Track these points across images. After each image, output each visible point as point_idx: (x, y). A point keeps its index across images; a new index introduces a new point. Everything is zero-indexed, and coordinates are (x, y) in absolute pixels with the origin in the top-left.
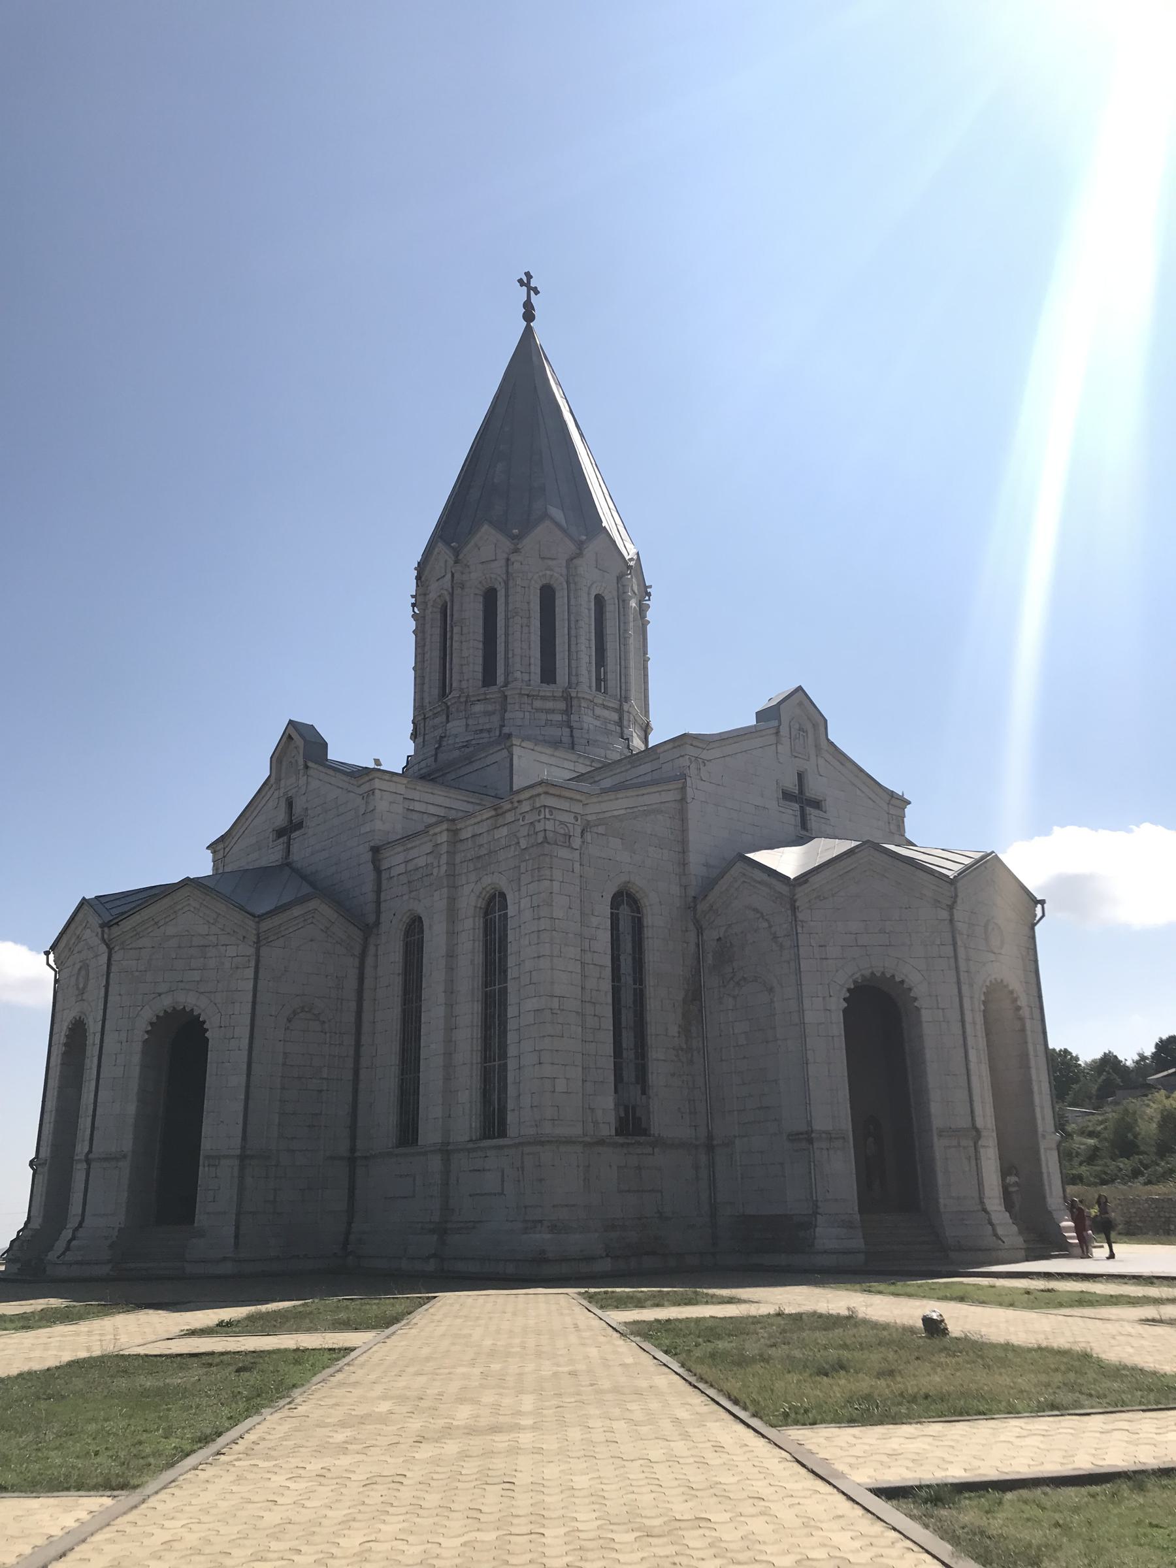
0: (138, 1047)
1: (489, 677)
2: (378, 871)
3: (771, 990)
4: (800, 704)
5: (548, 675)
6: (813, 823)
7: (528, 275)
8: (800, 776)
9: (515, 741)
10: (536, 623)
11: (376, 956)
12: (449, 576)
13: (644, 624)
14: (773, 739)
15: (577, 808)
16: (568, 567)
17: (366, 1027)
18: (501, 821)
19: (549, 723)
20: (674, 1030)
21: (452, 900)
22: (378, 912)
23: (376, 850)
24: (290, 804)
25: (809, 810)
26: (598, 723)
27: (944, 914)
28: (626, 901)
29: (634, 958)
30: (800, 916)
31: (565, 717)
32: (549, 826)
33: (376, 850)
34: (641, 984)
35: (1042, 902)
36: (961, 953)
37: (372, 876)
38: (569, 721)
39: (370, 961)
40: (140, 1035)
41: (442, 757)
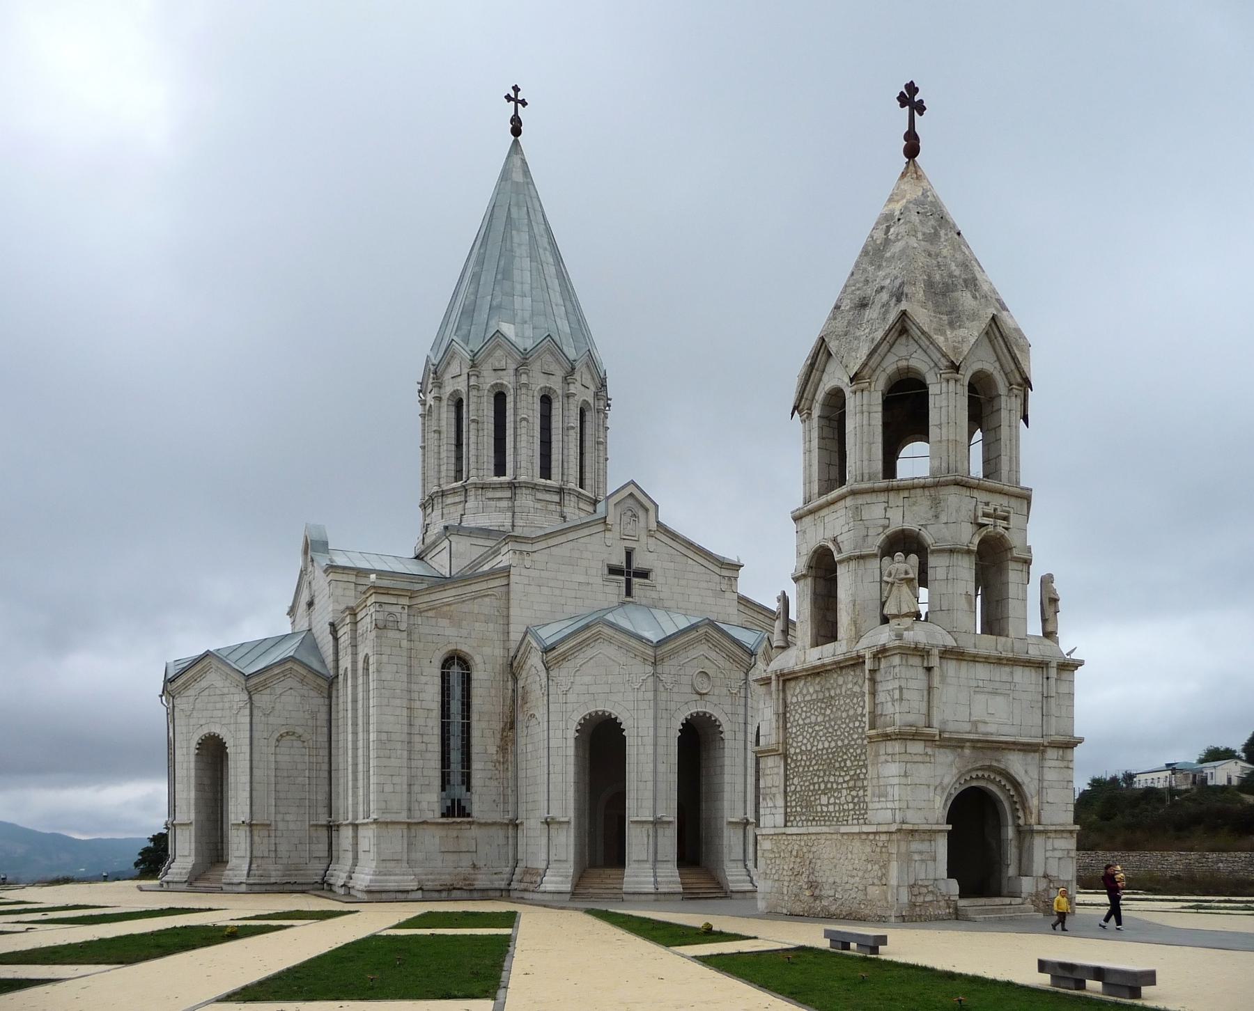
0: (193, 758)
1: (458, 477)
2: (336, 639)
4: (631, 495)
5: (500, 469)
6: (636, 590)
8: (629, 554)
14: (601, 527)
15: (405, 601)
19: (500, 510)
20: (492, 749)
21: (354, 663)
22: (337, 667)
23: (332, 625)
25: (635, 580)
26: (538, 505)
27: (650, 669)
28: (456, 662)
29: (463, 704)
32: (380, 616)
34: (469, 718)
36: (663, 696)
39: (334, 699)
40: (193, 751)
41: (428, 541)
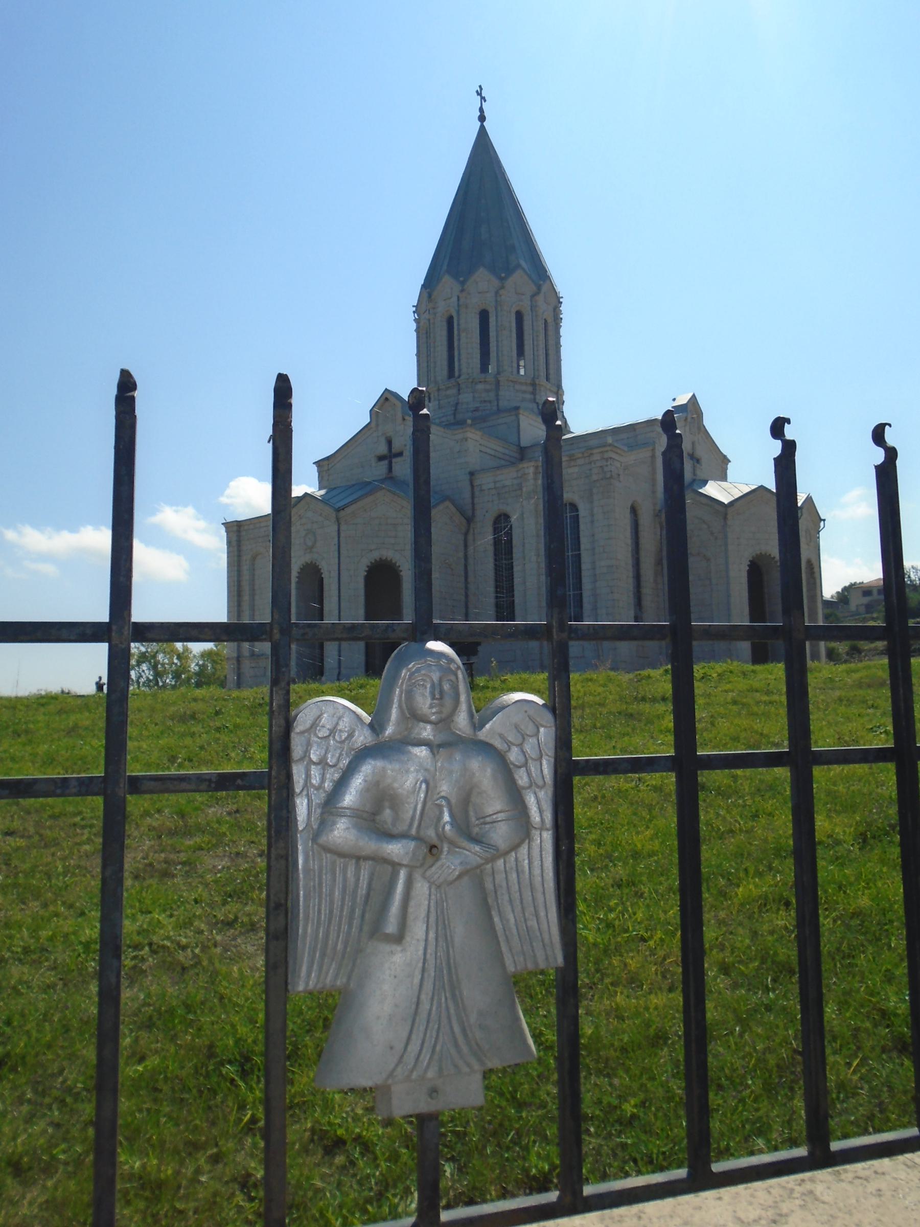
3: (708, 560)
7: (480, 87)
9: (521, 411)
10: (514, 335)
11: (474, 534)
12: (455, 299)
13: (558, 336)
16: (531, 301)
17: (470, 574)
18: (572, 463)
22: (473, 509)
23: (472, 474)
24: (389, 442)
30: (729, 523)
31: (532, 396)
33: (472, 474)
35: (824, 520)
37: (469, 488)
38: (535, 399)
39: (470, 537)
